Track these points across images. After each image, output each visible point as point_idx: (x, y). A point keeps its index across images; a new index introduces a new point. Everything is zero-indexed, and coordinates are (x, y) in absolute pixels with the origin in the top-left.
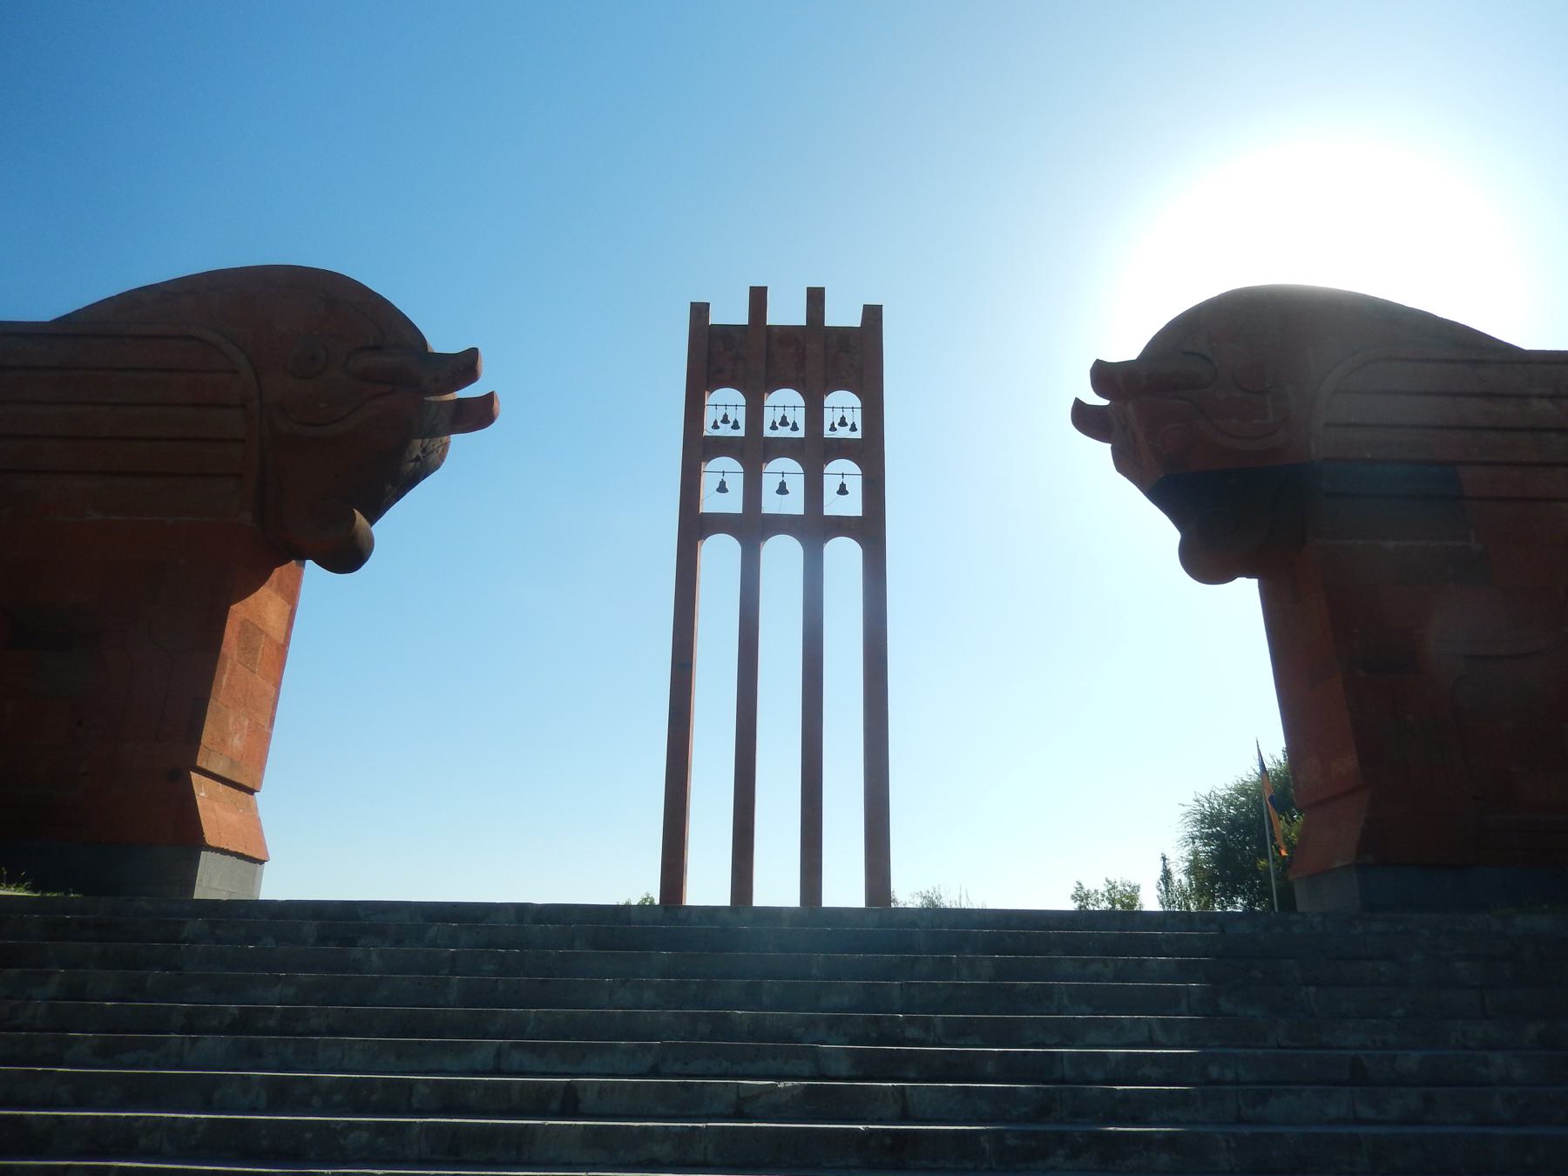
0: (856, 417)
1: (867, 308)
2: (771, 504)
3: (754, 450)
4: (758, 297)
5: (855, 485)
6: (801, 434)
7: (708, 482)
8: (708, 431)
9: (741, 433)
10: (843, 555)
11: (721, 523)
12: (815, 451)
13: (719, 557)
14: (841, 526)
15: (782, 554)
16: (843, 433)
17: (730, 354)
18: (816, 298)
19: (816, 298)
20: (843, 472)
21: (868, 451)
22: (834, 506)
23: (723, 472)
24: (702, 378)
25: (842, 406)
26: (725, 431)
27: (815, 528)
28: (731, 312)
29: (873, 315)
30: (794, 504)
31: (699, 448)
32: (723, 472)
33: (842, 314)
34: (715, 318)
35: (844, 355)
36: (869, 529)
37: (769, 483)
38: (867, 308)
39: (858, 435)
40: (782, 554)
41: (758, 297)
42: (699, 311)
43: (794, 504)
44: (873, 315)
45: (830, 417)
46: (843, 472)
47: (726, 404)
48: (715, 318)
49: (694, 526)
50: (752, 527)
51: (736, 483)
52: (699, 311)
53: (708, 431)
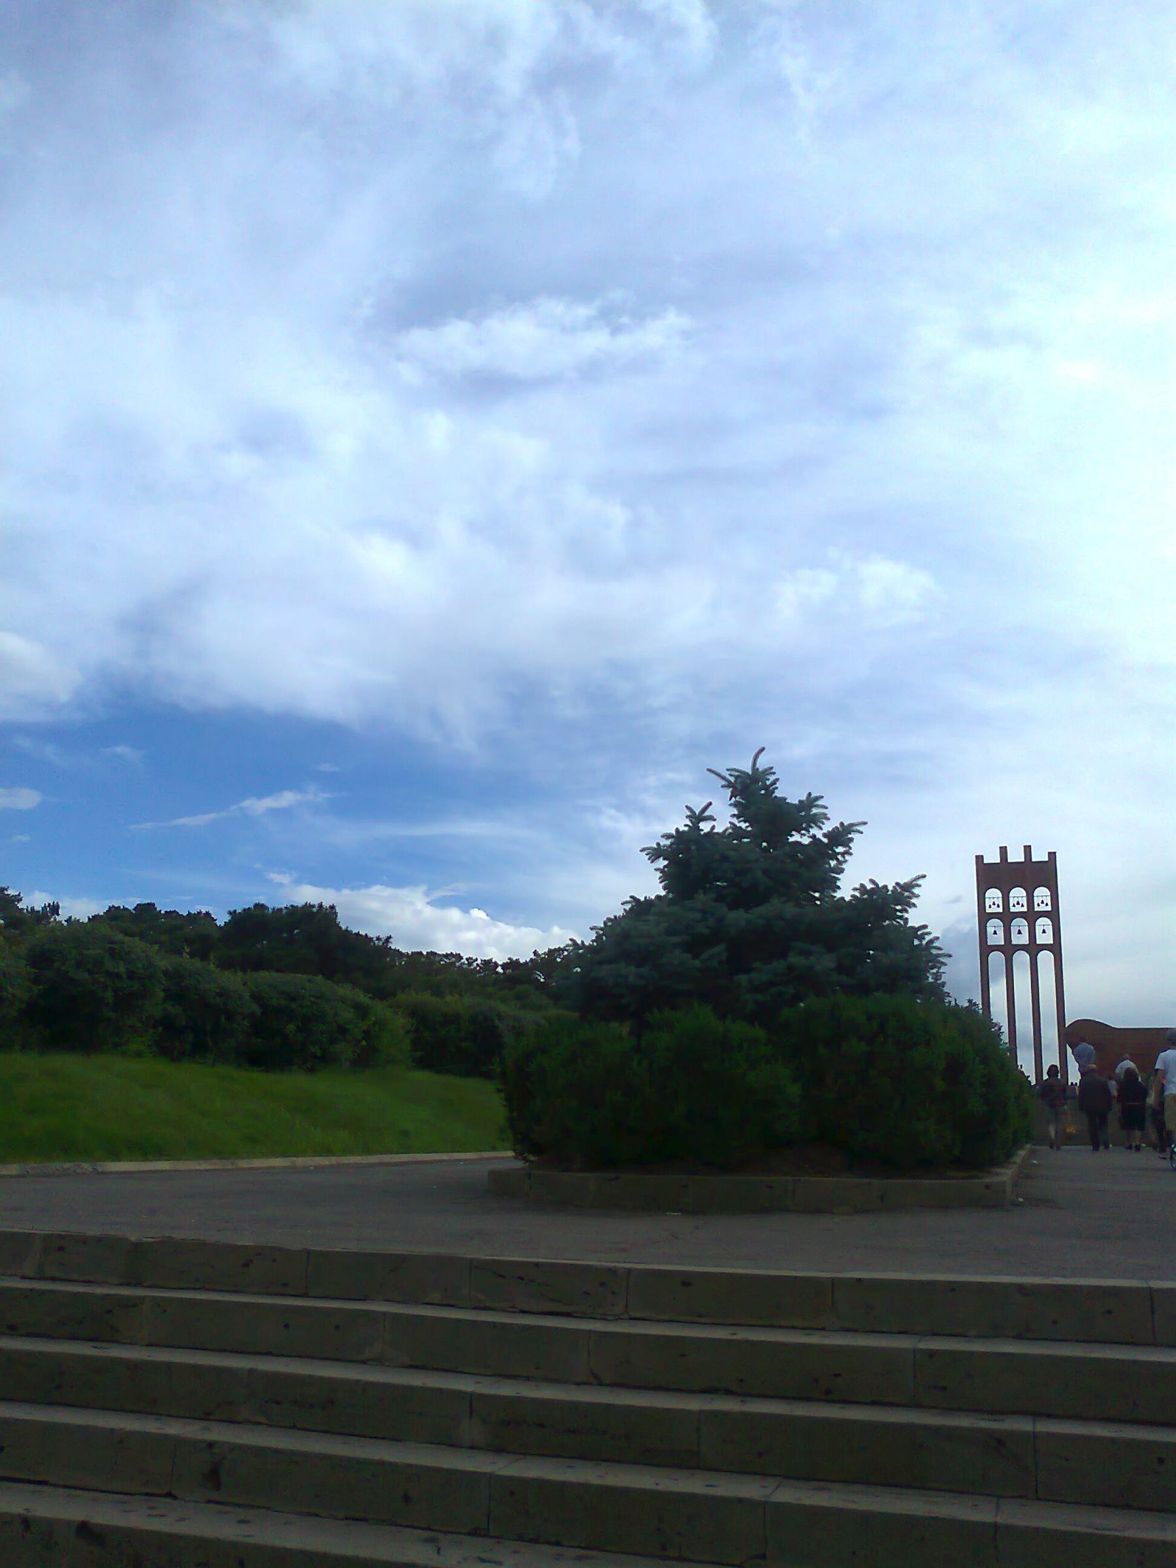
0: (1048, 900)
1: (1050, 853)
2: (1016, 940)
3: (1007, 917)
4: (1003, 851)
5: (1049, 930)
6: (1025, 909)
7: (990, 930)
8: (988, 910)
9: (1000, 910)
10: (1045, 958)
11: (997, 948)
12: (1031, 916)
13: (997, 959)
14: (1044, 947)
15: (1022, 958)
16: (1043, 908)
17: (994, 875)
18: (1028, 849)
19: (1028, 849)
20: (1043, 923)
21: (1054, 915)
22: (1041, 939)
23: (995, 925)
24: (982, 887)
25: (1042, 893)
26: (994, 909)
27: (1033, 949)
28: (993, 857)
29: (1052, 855)
30: (1024, 939)
31: (984, 917)
32: (995, 925)
33: (1039, 856)
34: (986, 861)
35: (1039, 873)
36: (1055, 948)
37: (1014, 931)
38: (1050, 853)
39: (1049, 908)
40: (1022, 958)
41: (1003, 851)
42: (979, 859)
43: (1024, 939)
44: (1052, 855)
45: (1037, 901)
46: (1043, 923)
47: (994, 895)
48: (986, 861)
49: (986, 950)
50: (1009, 950)
51: (1001, 933)
52: (979, 859)
53: (988, 910)
